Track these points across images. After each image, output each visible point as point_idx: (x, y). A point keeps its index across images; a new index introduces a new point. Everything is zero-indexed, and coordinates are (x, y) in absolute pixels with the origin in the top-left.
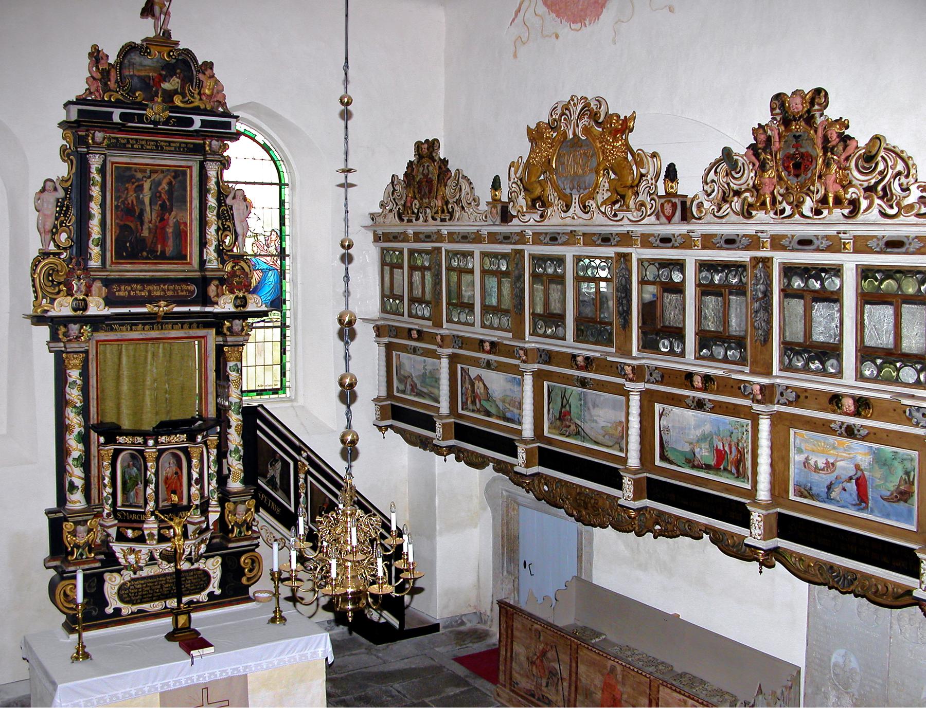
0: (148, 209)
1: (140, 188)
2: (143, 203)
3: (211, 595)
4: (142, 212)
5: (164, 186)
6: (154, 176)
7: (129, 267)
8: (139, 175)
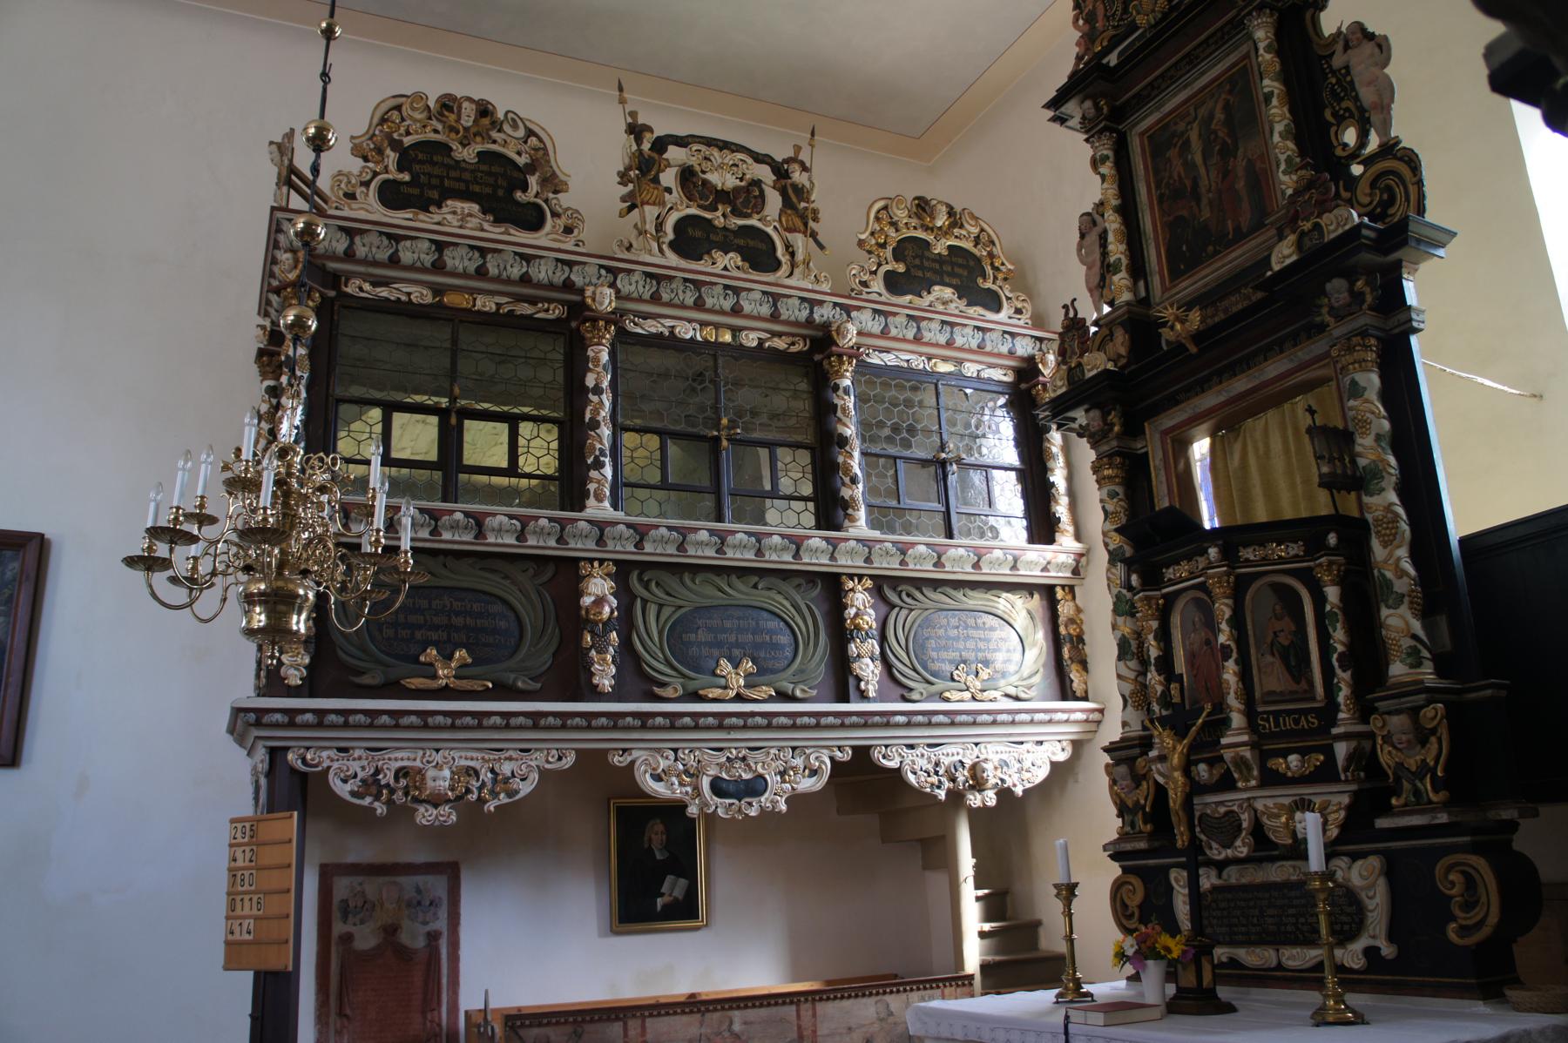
0: (1202, 171)
1: (1187, 143)
2: (1194, 166)
3: (1371, 953)
4: (1195, 180)
5: (1219, 116)
6: (1202, 112)
7: (1184, 284)
8: (1181, 126)
